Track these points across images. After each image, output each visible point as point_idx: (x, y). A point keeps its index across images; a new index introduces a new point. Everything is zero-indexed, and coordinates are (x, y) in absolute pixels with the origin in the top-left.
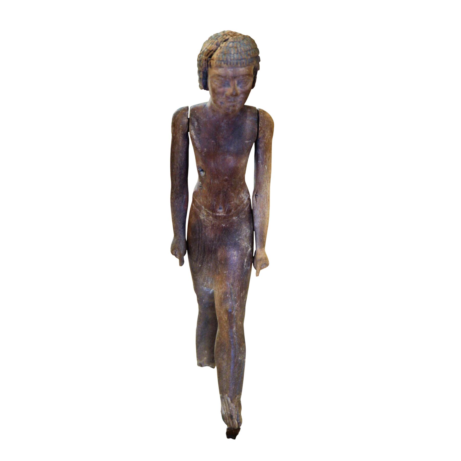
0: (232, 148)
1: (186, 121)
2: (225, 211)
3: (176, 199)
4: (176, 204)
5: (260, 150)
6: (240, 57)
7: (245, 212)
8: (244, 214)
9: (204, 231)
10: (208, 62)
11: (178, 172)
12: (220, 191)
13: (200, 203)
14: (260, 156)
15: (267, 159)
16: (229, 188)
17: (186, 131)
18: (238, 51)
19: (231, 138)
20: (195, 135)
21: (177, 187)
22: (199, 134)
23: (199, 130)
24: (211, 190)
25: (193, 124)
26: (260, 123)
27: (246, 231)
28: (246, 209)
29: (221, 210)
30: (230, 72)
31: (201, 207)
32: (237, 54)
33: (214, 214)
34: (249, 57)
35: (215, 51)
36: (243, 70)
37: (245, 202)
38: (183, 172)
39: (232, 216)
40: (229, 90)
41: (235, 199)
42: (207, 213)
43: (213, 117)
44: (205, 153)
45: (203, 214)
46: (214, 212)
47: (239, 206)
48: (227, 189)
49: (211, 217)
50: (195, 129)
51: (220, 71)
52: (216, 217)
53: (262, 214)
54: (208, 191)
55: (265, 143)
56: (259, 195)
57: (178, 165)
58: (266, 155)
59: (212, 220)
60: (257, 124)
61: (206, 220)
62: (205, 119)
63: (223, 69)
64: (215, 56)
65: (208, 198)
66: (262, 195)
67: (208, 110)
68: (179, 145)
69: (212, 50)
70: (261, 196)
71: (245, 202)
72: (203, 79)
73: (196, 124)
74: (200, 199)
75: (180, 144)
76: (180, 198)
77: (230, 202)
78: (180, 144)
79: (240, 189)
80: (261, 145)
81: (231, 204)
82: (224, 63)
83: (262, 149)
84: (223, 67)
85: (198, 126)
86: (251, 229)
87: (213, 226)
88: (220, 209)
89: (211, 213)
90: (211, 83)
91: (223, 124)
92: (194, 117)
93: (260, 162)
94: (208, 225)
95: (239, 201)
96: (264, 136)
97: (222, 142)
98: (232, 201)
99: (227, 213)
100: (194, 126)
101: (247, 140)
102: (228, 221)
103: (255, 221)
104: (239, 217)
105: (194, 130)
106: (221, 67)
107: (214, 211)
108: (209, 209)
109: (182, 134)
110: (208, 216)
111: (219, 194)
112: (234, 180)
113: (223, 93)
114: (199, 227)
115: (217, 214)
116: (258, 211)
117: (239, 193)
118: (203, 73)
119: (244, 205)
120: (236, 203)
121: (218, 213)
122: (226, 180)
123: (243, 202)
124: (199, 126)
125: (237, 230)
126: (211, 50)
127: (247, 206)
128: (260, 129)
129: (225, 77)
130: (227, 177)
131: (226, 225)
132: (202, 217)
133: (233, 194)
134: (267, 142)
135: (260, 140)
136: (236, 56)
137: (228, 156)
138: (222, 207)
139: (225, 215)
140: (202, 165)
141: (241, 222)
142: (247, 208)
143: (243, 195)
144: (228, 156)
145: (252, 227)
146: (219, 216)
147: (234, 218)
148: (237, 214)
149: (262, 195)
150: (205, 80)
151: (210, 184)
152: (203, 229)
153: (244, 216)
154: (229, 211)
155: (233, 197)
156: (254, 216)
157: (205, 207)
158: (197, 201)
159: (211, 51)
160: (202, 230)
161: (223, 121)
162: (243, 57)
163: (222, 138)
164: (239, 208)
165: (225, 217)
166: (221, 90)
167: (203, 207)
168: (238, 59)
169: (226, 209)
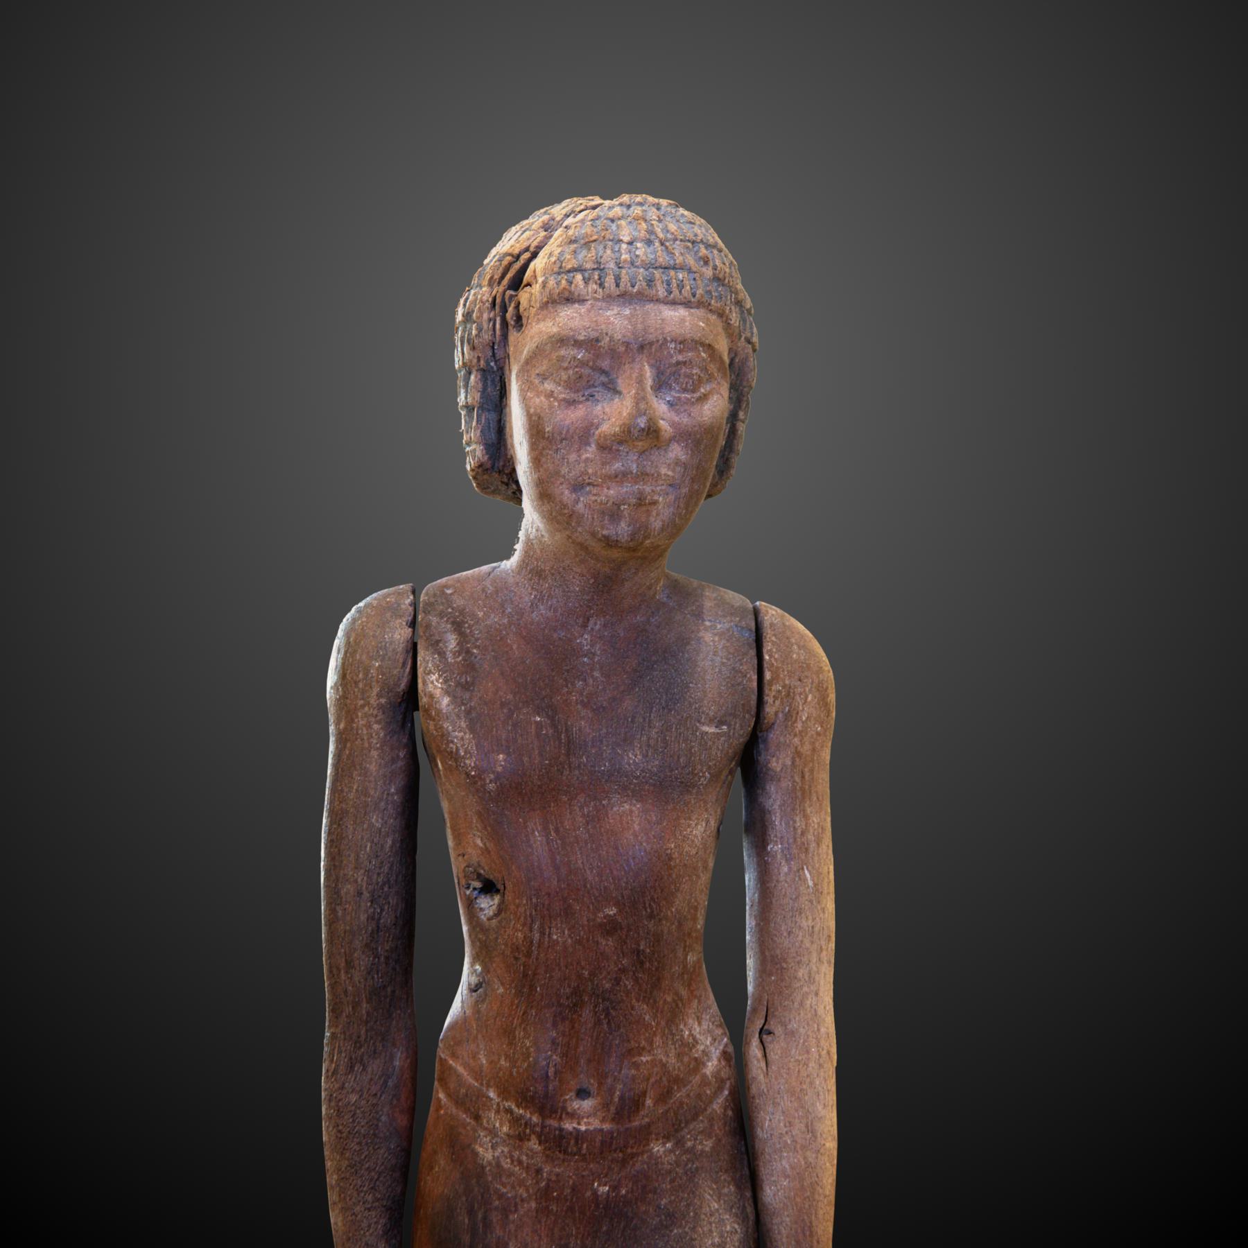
0: (633, 757)
1: (400, 634)
2: (606, 1106)
3: (351, 1068)
4: (353, 1098)
5: (772, 788)
6: (663, 258)
7: (711, 1120)
8: (708, 1133)
9: (498, 1232)
10: (504, 309)
11: (363, 917)
12: (576, 992)
13: (478, 1074)
14: (777, 821)
15: (810, 837)
16: (623, 970)
17: (403, 685)
18: (651, 232)
19: (628, 704)
20: (447, 692)
21: (356, 1005)
22: (466, 687)
23: (469, 666)
24: (532, 988)
25: (436, 646)
26: (767, 647)
27: (721, 1222)
28: (718, 1105)
29: (587, 1104)
30: (617, 321)
31: (481, 1095)
32: (649, 242)
33: (553, 1123)
34: (708, 272)
35: (534, 255)
36: (683, 320)
37: (711, 1066)
38: (387, 919)
39: (644, 1135)
40: (612, 413)
41: (658, 1040)
42: (515, 1121)
43: (533, 606)
44: (498, 777)
45: (492, 1132)
46: (553, 1111)
47: (678, 1081)
48: (617, 981)
49: (534, 1144)
50: (445, 670)
51: (569, 318)
52: (558, 1143)
53: (799, 1127)
54: (519, 993)
55: (798, 753)
56: (779, 1030)
57: (360, 876)
58: (806, 817)
59: (538, 1160)
60: (753, 652)
61: (506, 1164)
62: (494, 619)
63: (583, 309)
64: (538, 264)
65: (519, 1033)
66: (793, 1025)
67: (511, 580)
68: (365, 773)
69: (527, 249)
70: (792, 1034)
71: (711, 1066)
72: (481, 407)
73: (452, 642)
74: (474, 1056)
75: (373, 767)
76: (375, 1066)
77: (630, 1052)
78: (373, 767)
79: (684, 993)
80: (775, 765)
81: (636, 1066)
82: (586, 281)
83: (785, 784)
84: (582, 301)
85: (463, 649)
86: (745, 1219)
87: (545, 1195)
88: (582, 1094)
89: (535, 1119)
90: (522, 392)
91: (585, 640)
92: (441, 615)
93: (775, 848)
94: (522, 1192)
95: (679, 1056)
96: (790, 716)
97: (583, 724)
98: (640, 1051)
99: (618, 1117)
100: (442, 654)
101: (711, 721)
102: (624, 1163)
103: (764, 1172)
104: (679, 1143)
105: (442, 672)
106: (569, 299)
107: (548, 1106)
108: (525, 1099)
109: (380, 707)
110: (522, 1138)
111: (577, 1006)
112: (651, 925)
113: (584, 434)
114: (471, 1212)
115: (569, 1126)
116: (779, 1116)
117: (674, 1015)
118: (484, 372)
119: (705, 1082)
120: (664, 1065)
121: (572, 1115)
122: (610, 928)
123: (699, 1063)
124: (468, 652)
125: (672, 1218)
126: (516, 251)
127: (720, 1089)
128: (768, 675)
129: (591, 344)
130: (612, 911)
131: (615, 1188)
132: (486, 1153)
133: (643, 1009)
134: (806, 749)
135: (772, 736)
136: (641, 250)
137: (615, 798)
138: (592, 1084)
139: (606, 1126)
140: (486, 851)
141: (692, 1175)
142: (721, 1100)
143: (697, 1029)
144: (615, 798)
145: (750, 1210)
146: (578, 1136)
147: (657, 1148)
148: (673, 1131)
149: (793, 1025)
150: (493, 416)
151: (528, 954)
152: (495, 1217)
153: (708, 1145)
154: (630, 1105)
155: (648, 1027)
156: (758, 1145)
157: (504, 1093)
158: (460, 1069)
159: (518, 257)
160: (487, 1225)
161: (585, 626)
162: (679, 259)
163: (585, 705)
164: (679, 1095)
165: (607, 1144)
166: (575, 415)
167: (492, 1094)
168: (651, 266)
169: (611, 1091)
